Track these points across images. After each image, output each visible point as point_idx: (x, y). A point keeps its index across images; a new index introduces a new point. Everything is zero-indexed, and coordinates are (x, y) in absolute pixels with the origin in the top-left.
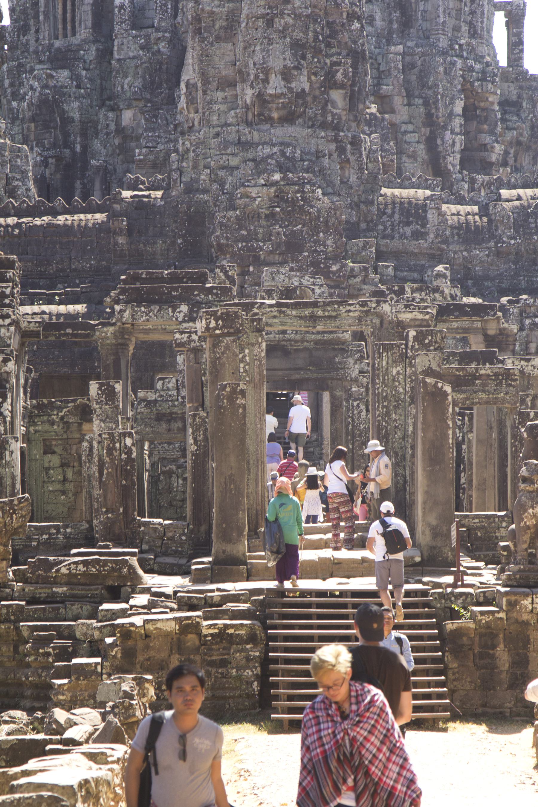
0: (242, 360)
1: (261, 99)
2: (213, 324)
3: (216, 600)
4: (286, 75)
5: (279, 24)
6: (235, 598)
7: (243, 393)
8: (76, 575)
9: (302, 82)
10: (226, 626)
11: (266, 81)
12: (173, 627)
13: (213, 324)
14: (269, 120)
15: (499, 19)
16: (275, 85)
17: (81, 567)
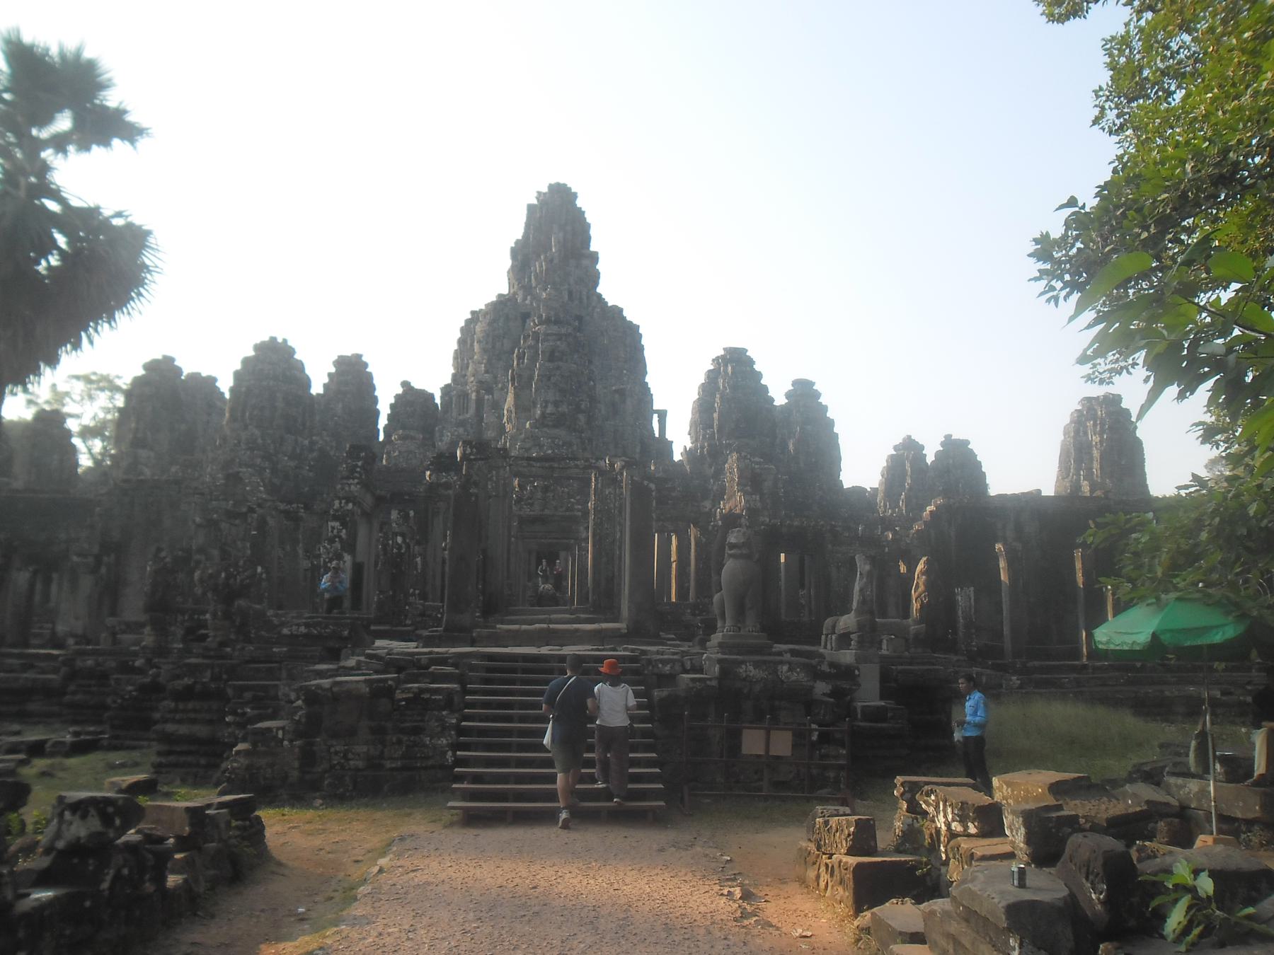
0: (491, 479)
1: (543, 415)
2: (469, 450)
3: (424, 662)
4: (556, 404)
5: (553, 380)
6: (442, 661)
7: (476, 484)
8: (297, 636)
9: (564, 408)
10: (422, 691)
11: (546, 407)
12: (365, 689)
13: (469, 450)
14: (547, 426)
15: (655, 417)
16: (550, 409)
17: (303, 629)
